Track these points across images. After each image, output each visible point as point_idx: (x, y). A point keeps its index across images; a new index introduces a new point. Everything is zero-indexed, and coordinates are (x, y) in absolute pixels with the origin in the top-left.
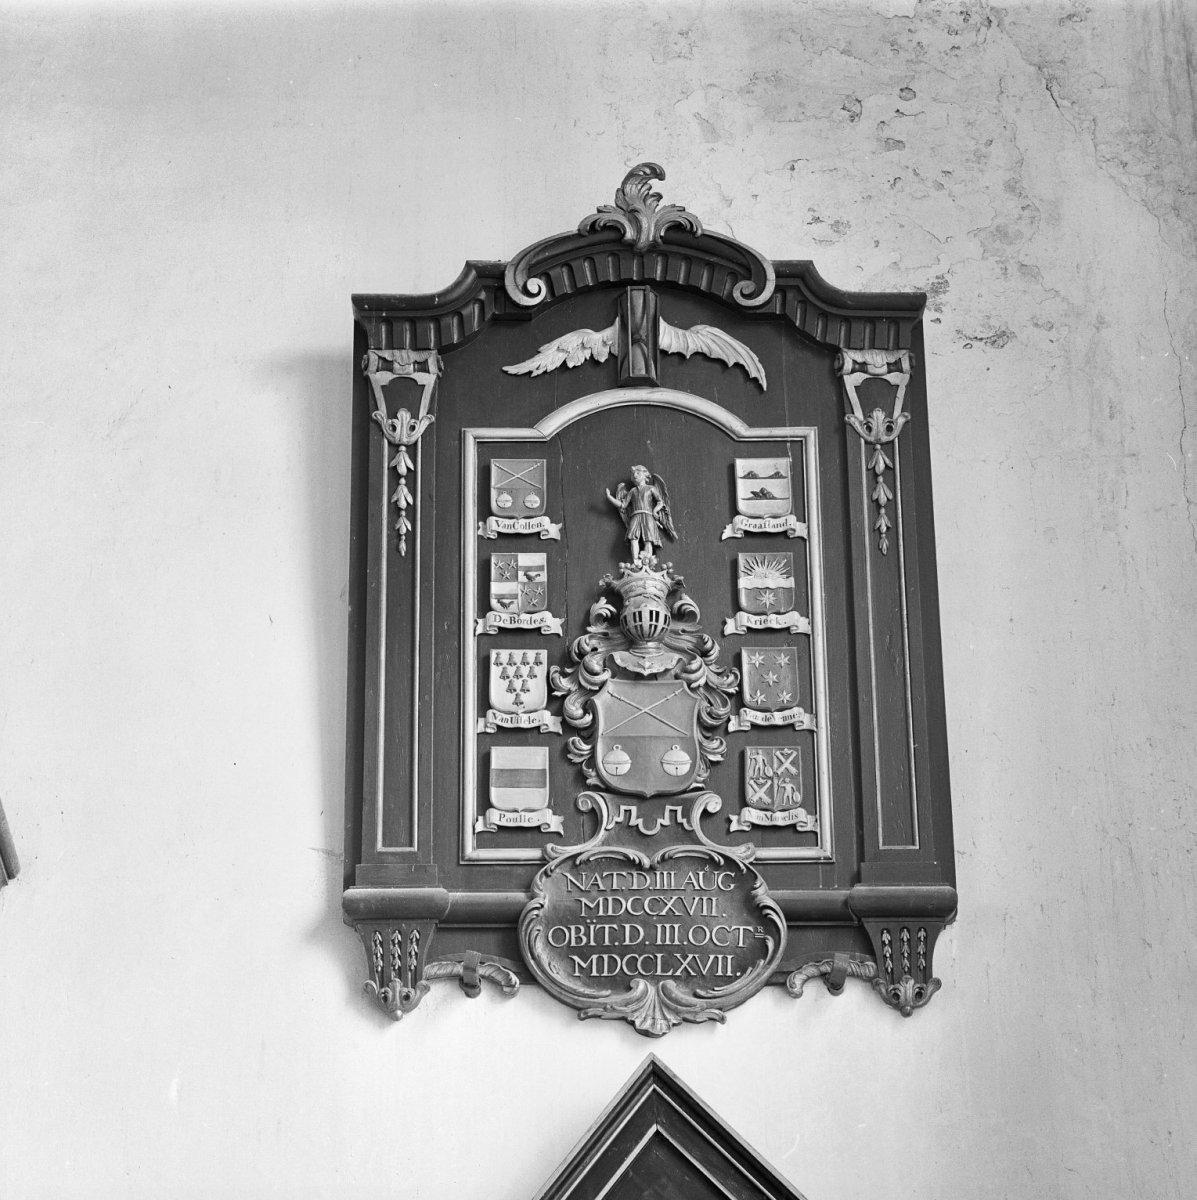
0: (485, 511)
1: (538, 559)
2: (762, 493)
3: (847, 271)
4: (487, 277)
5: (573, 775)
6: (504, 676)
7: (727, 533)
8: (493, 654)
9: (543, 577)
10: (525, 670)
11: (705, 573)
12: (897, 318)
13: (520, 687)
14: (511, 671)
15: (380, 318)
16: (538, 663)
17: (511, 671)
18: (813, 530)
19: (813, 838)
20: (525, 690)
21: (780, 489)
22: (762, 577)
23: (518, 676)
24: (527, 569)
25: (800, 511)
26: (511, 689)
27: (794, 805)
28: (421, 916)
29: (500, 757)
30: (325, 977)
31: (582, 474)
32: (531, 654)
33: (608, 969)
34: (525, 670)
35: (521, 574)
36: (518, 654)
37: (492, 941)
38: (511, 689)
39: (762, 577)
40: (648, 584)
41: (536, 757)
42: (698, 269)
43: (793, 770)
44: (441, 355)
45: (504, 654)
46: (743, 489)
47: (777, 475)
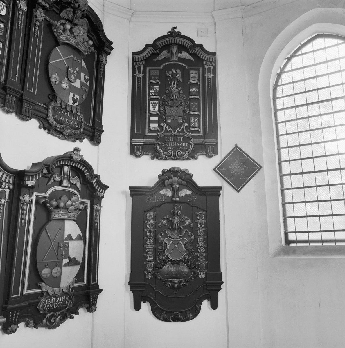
0: (150, 79)
1: (157, 86)
6: (152, 105)
7: (188, 83)
8: (151, 102)
9: (158, 90)
10: (155, 104)
14: (153, 104)
16: (157, 103)
17: (153, 104)
18: (201, 84)
19: (200, 132)
20: (155, 107)
21: (197, 76)
22: (194, 90)
23: (154, 105)
24: (156, 88)
25: (199, 80)
26: (153, 107)
29: (152, 119)
32: (156, 102)
34: (155, 104)
35: (155, 89)
36: (154, 102)
38: (153, 107)
41: (156, 119)
43: (197, 121)
45: (152, 102)
46: (191, 75)
47: (195, 73)
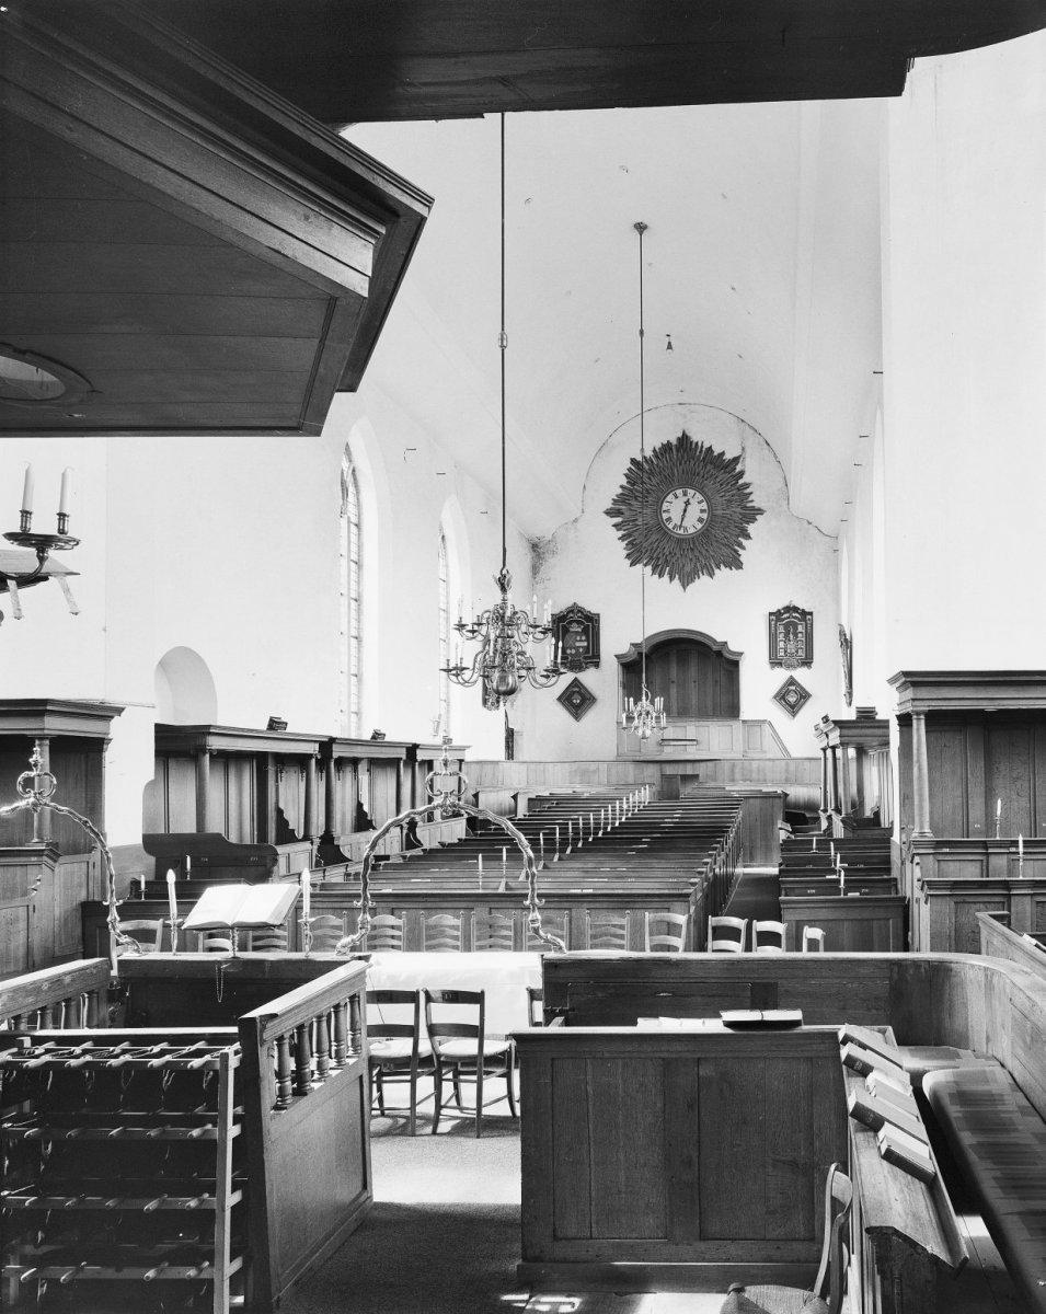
2: (800, 628)
3: (807, 610)
4: (779, 611)
5: (786, 652)
11: (796, 635)
12: (811, 614)
13: (782, 644)
15: (771, 614)
27: (801, 653)
28: (775, 662)
30: (768, 666)
31: (786, 627)
33: (789, 666)
37: (780, 664)
39: (800, 635)
40: (791, 636)
42: (795, 609)
44: (776, 616)
